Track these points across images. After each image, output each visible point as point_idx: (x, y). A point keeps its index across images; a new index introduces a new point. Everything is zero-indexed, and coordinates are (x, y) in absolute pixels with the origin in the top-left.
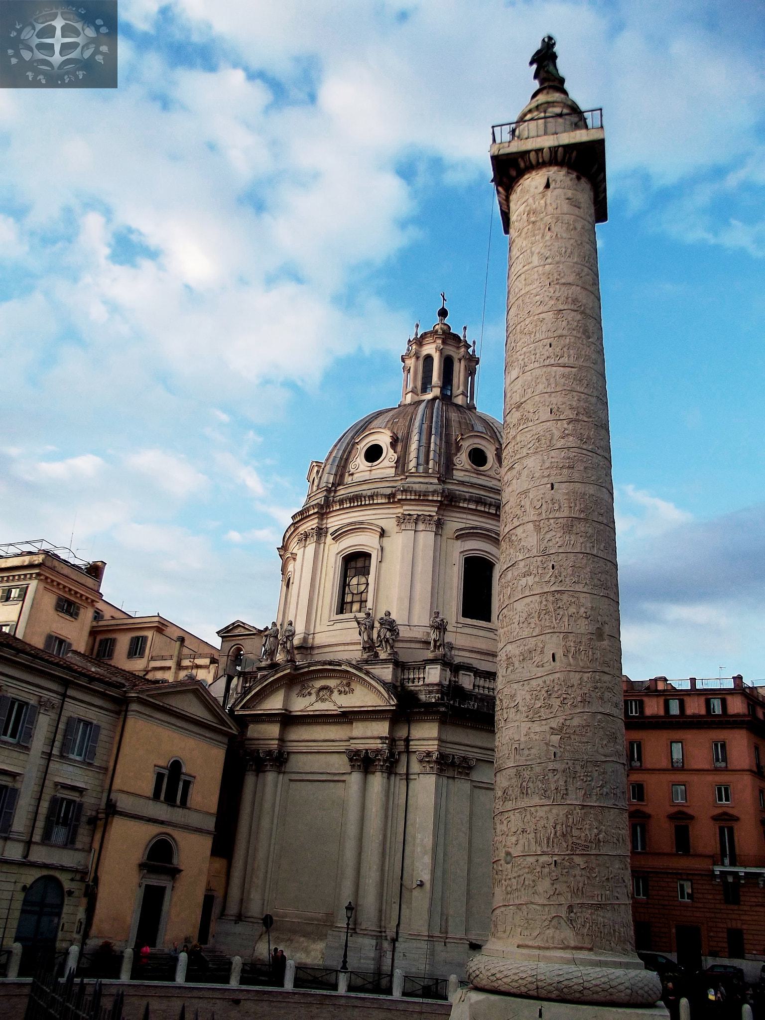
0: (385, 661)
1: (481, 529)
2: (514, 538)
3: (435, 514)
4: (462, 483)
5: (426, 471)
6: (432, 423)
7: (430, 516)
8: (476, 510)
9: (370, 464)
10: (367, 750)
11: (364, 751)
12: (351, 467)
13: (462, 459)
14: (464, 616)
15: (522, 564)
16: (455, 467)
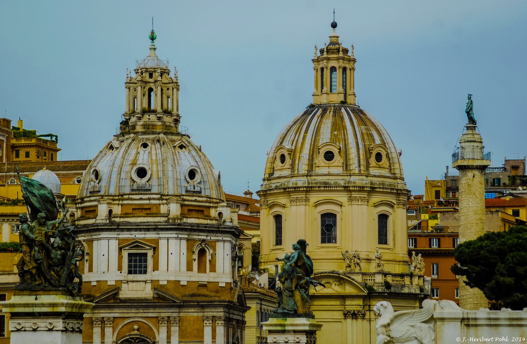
0: (358, 273)
1: (385, 201)
2: (466, 288)
3: (366, 196)
4: (375, 176)
5: (360, 170)
6: (357, 139)
7: (364, 197)
8: (383, 191)
9: (327, 162)
10: (354, 310)
11: (353, 311)
12: (316, 161)
13: (373, 160)
14: (379, 243)
15: (468, 295)
16: (370, 166)
